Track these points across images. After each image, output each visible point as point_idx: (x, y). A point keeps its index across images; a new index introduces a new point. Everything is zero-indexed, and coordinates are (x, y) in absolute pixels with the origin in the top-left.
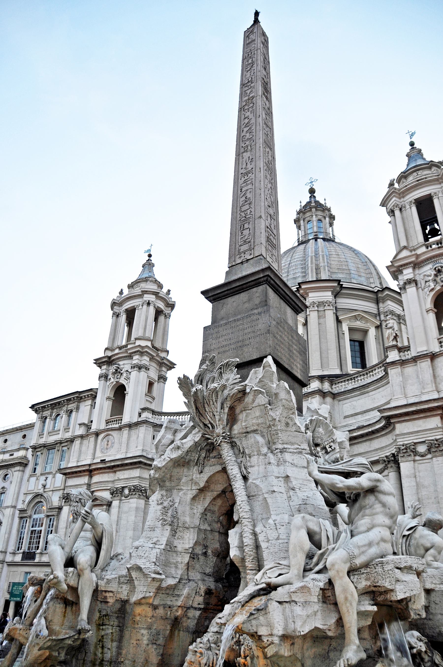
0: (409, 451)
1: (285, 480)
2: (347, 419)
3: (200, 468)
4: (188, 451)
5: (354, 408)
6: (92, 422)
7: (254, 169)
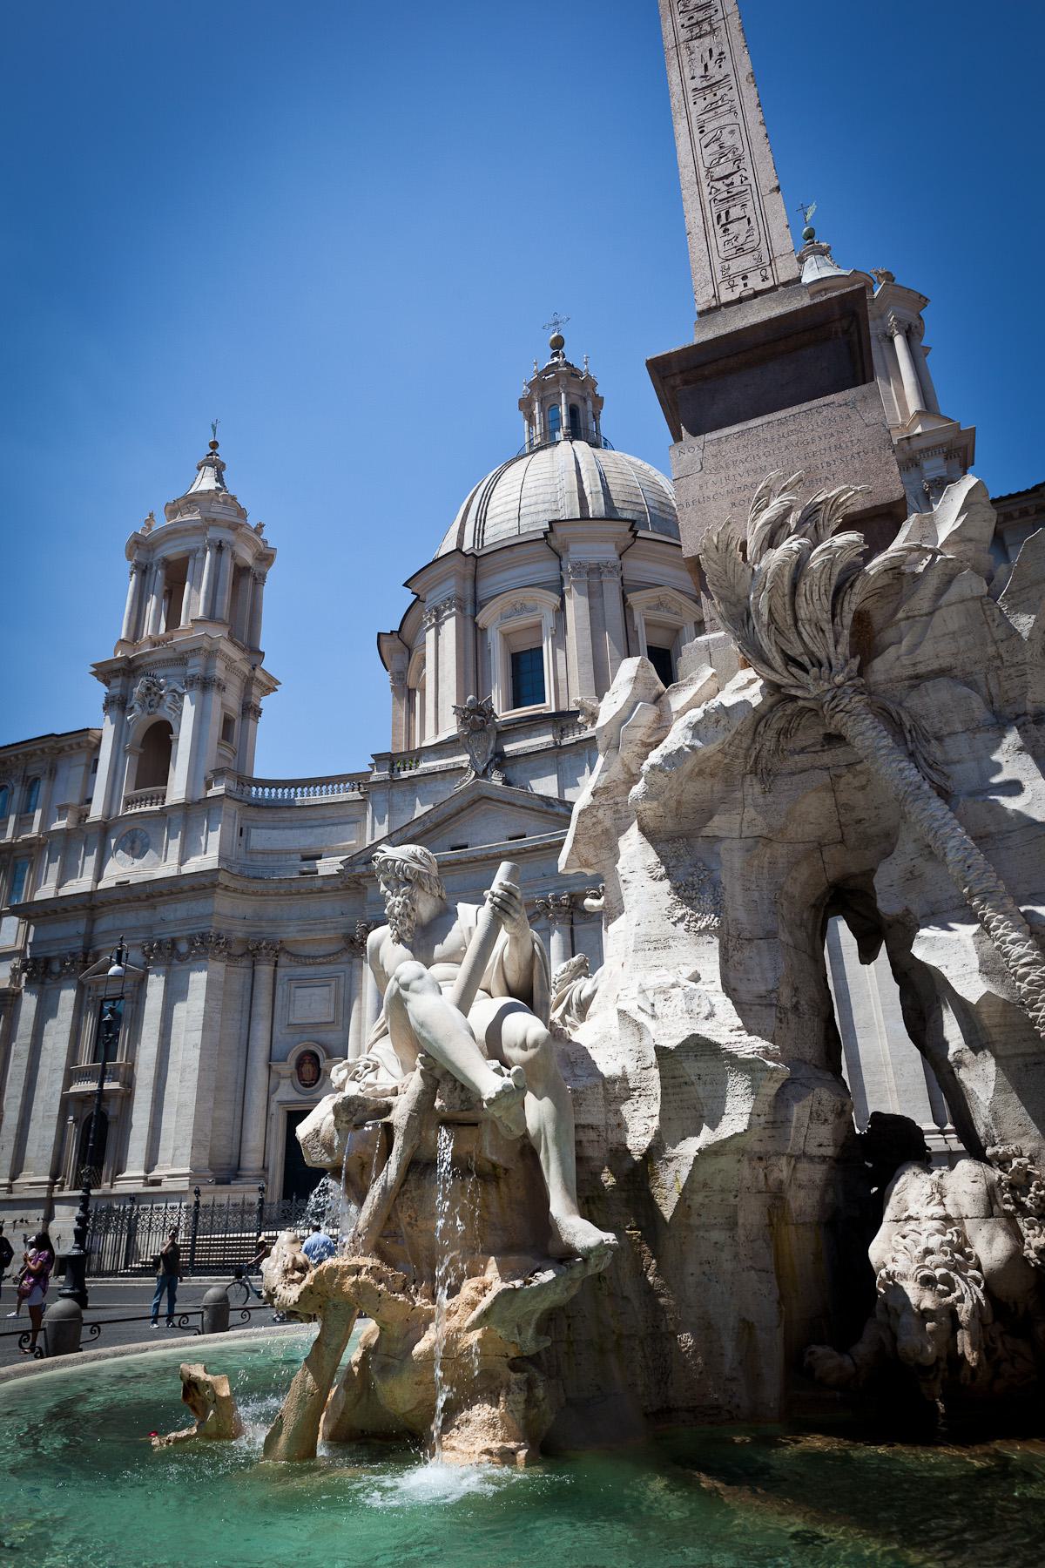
7: (732, 77)
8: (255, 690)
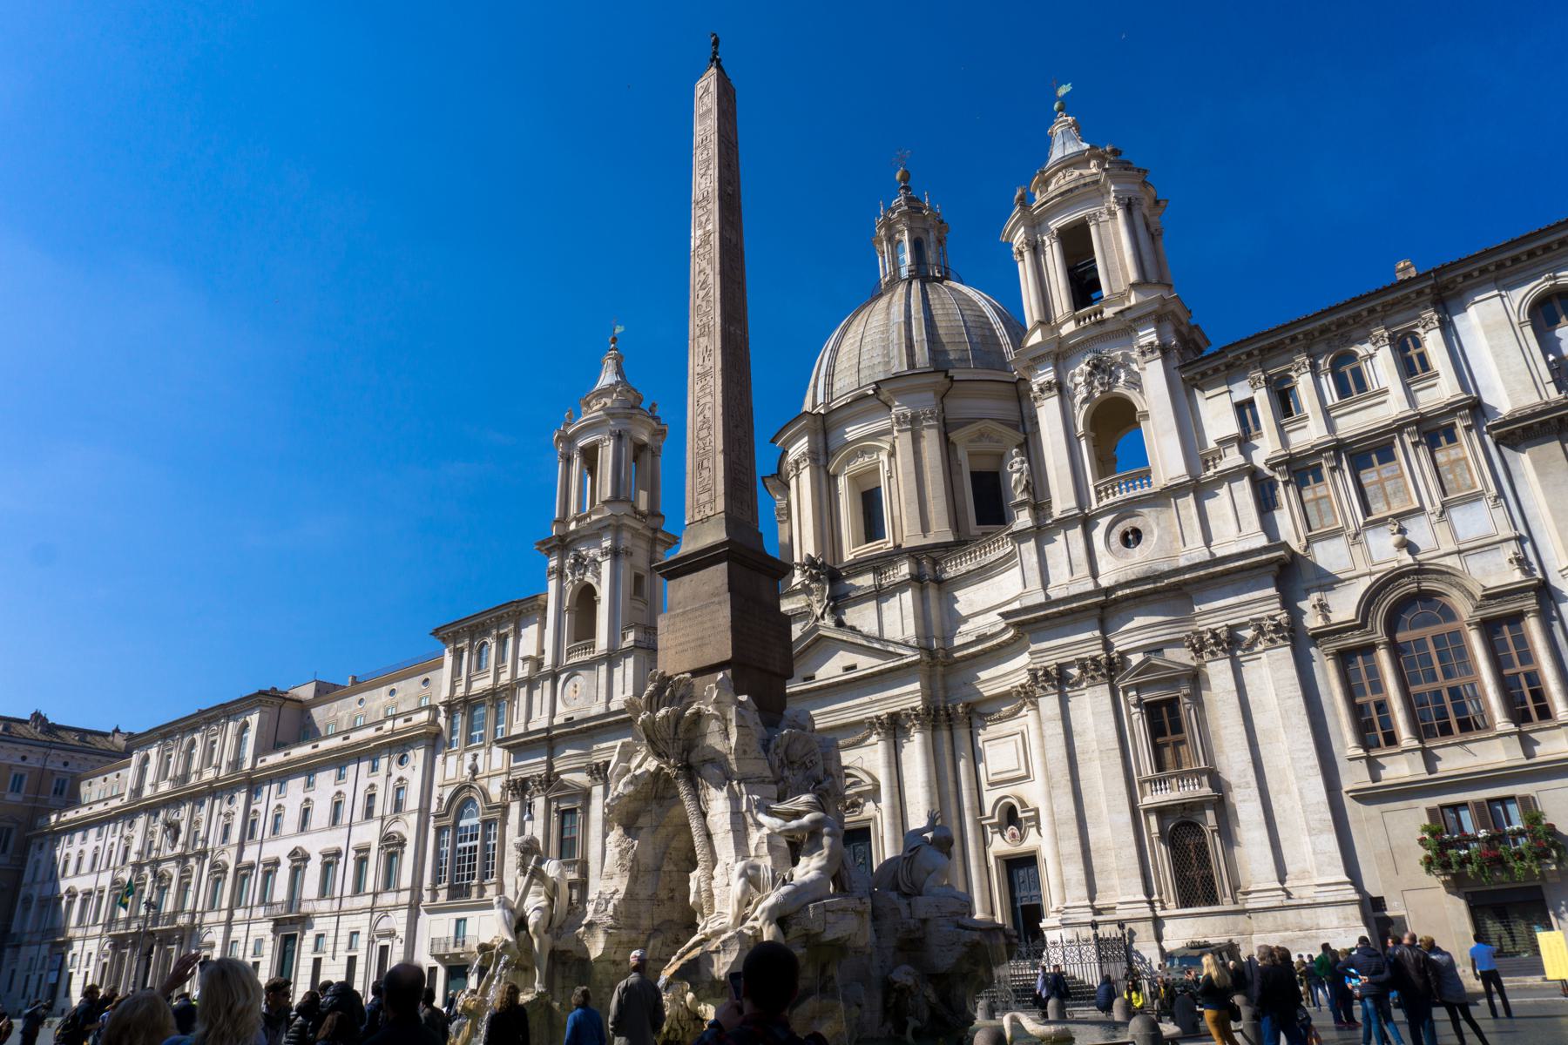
5: (971, 605)
6: (543, 652)
8: (659, 549)
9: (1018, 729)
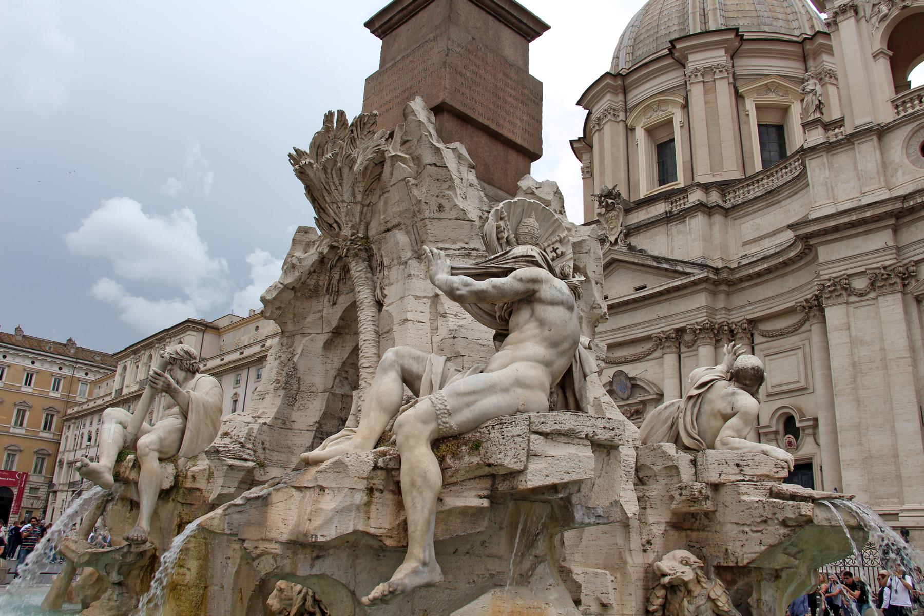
0: (838, 288)
1: (433, 302)
2: (748, 246)
3: (331, 298)
4: (310, 273)
9: (798, 344)
